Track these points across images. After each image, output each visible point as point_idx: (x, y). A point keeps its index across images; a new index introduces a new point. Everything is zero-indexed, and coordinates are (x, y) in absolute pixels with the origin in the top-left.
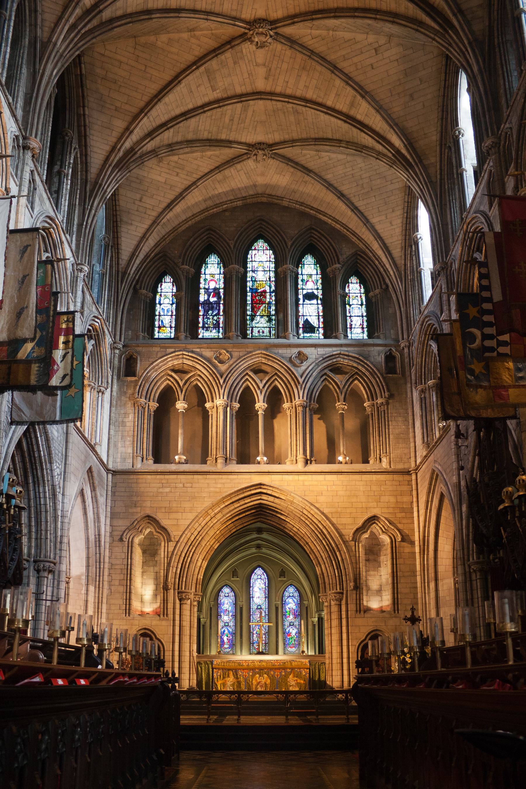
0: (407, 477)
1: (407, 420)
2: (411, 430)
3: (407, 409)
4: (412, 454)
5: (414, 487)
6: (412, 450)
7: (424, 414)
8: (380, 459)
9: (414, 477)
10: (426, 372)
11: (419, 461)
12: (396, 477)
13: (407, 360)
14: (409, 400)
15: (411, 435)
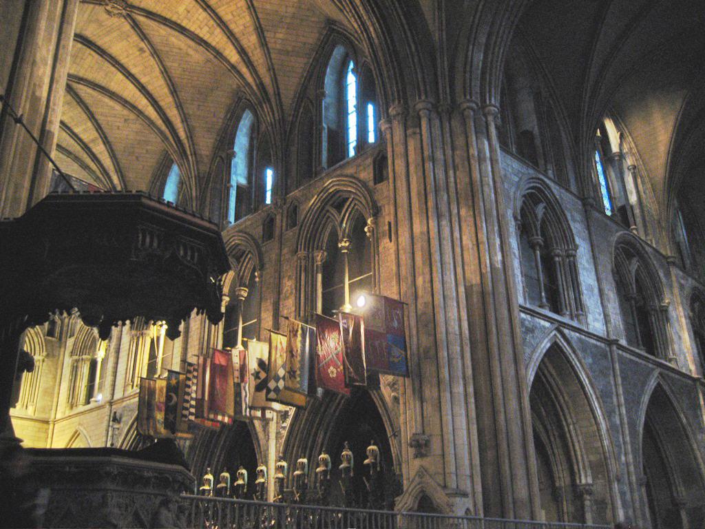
0: (45, 426)
1: (55, 378)
2: (57, 387)
3: (57, 369)
4: (54, 408)
5: (50, 435)
6: (55, 404)
7: (73, 380)
8: (27, 406)
9: (51, 426)
10: (83, 347)
11: (59, 416)
12: (37, 424)
13: (65, 329)
14: (60, 363)
15: (56, 391)
